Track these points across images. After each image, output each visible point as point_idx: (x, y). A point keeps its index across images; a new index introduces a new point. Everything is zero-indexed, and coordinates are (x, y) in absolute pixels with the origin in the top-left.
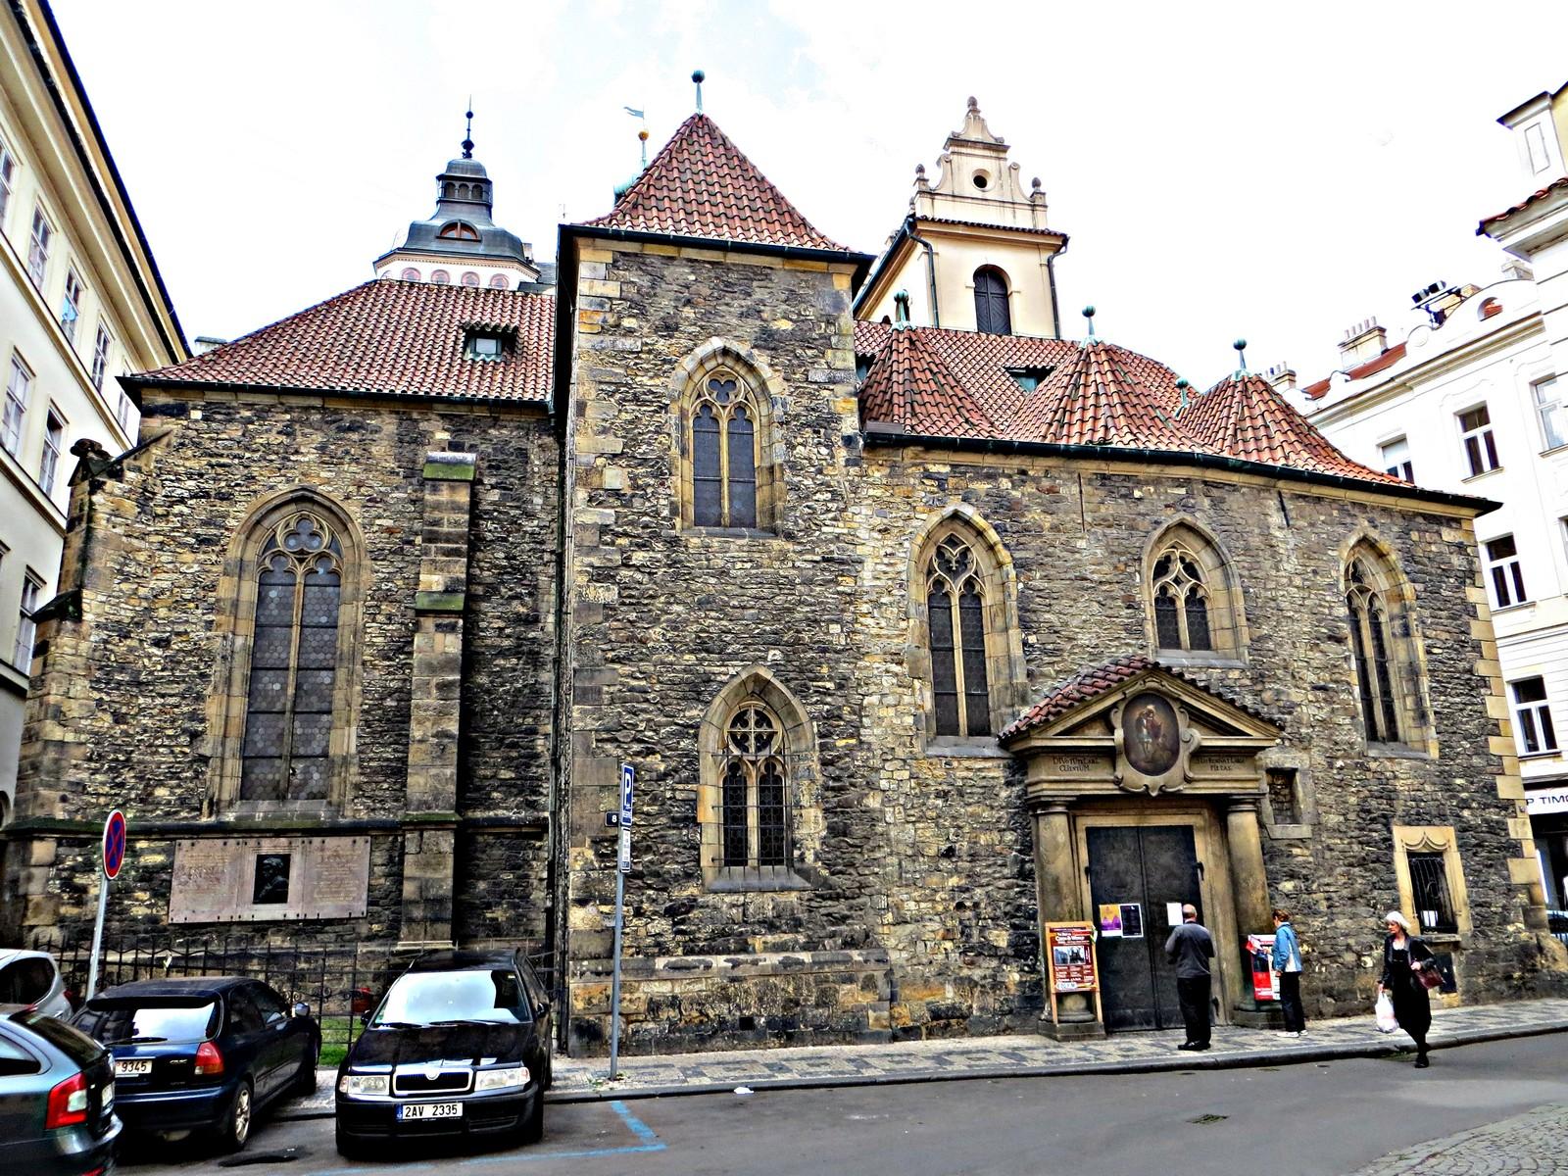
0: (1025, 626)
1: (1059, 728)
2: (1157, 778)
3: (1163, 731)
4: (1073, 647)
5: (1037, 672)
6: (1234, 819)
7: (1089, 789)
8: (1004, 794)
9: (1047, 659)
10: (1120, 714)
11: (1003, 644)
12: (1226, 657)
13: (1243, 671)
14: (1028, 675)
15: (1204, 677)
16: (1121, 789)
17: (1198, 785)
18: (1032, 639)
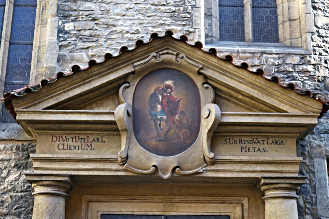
0: (63, 14)
1: (52, 102)
2: (170, 158)
3: (181, 107)
4: (110, 33)
5: (68, 57)
6: (271, 207)
7: (86, 170)
8: (12, 177)
9: (81, 44)
10: (131, 90)
11: (45, 34)
12: (291, 46)
13: (303, 57)
14: (58, 61)
15: (257, 62)
16: (126, 170)
17: (221, 167)
18: (69, 26)
